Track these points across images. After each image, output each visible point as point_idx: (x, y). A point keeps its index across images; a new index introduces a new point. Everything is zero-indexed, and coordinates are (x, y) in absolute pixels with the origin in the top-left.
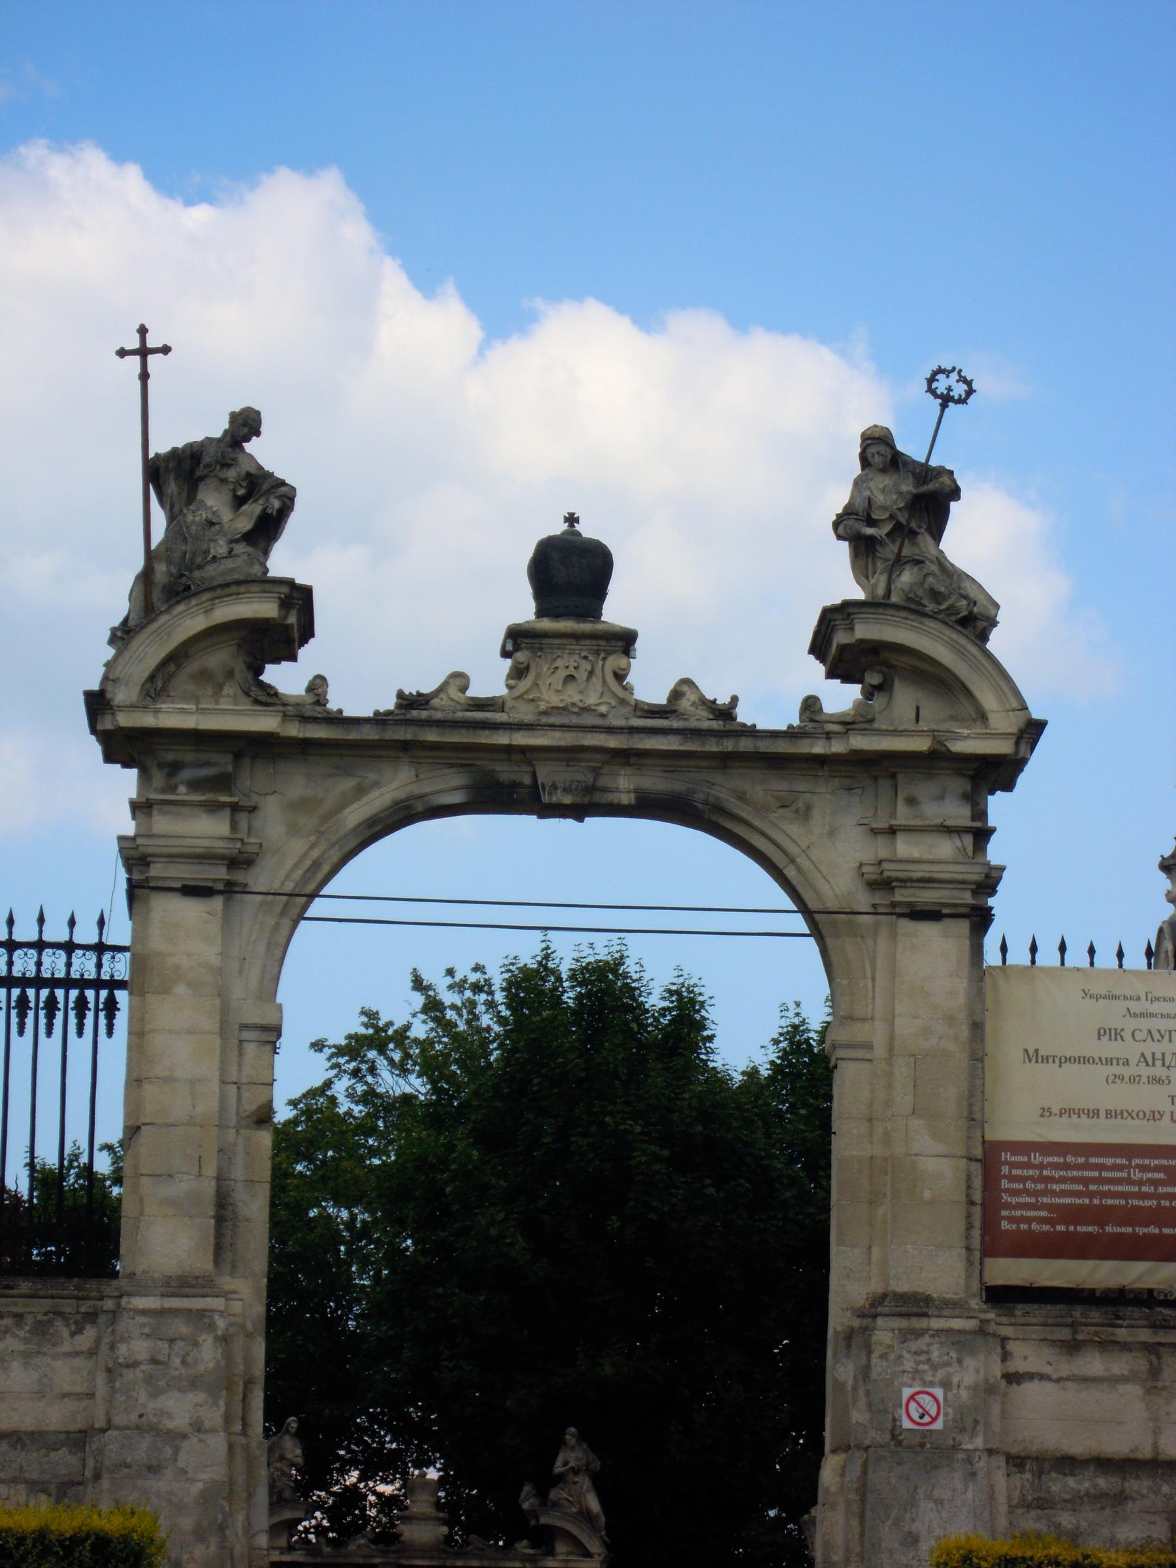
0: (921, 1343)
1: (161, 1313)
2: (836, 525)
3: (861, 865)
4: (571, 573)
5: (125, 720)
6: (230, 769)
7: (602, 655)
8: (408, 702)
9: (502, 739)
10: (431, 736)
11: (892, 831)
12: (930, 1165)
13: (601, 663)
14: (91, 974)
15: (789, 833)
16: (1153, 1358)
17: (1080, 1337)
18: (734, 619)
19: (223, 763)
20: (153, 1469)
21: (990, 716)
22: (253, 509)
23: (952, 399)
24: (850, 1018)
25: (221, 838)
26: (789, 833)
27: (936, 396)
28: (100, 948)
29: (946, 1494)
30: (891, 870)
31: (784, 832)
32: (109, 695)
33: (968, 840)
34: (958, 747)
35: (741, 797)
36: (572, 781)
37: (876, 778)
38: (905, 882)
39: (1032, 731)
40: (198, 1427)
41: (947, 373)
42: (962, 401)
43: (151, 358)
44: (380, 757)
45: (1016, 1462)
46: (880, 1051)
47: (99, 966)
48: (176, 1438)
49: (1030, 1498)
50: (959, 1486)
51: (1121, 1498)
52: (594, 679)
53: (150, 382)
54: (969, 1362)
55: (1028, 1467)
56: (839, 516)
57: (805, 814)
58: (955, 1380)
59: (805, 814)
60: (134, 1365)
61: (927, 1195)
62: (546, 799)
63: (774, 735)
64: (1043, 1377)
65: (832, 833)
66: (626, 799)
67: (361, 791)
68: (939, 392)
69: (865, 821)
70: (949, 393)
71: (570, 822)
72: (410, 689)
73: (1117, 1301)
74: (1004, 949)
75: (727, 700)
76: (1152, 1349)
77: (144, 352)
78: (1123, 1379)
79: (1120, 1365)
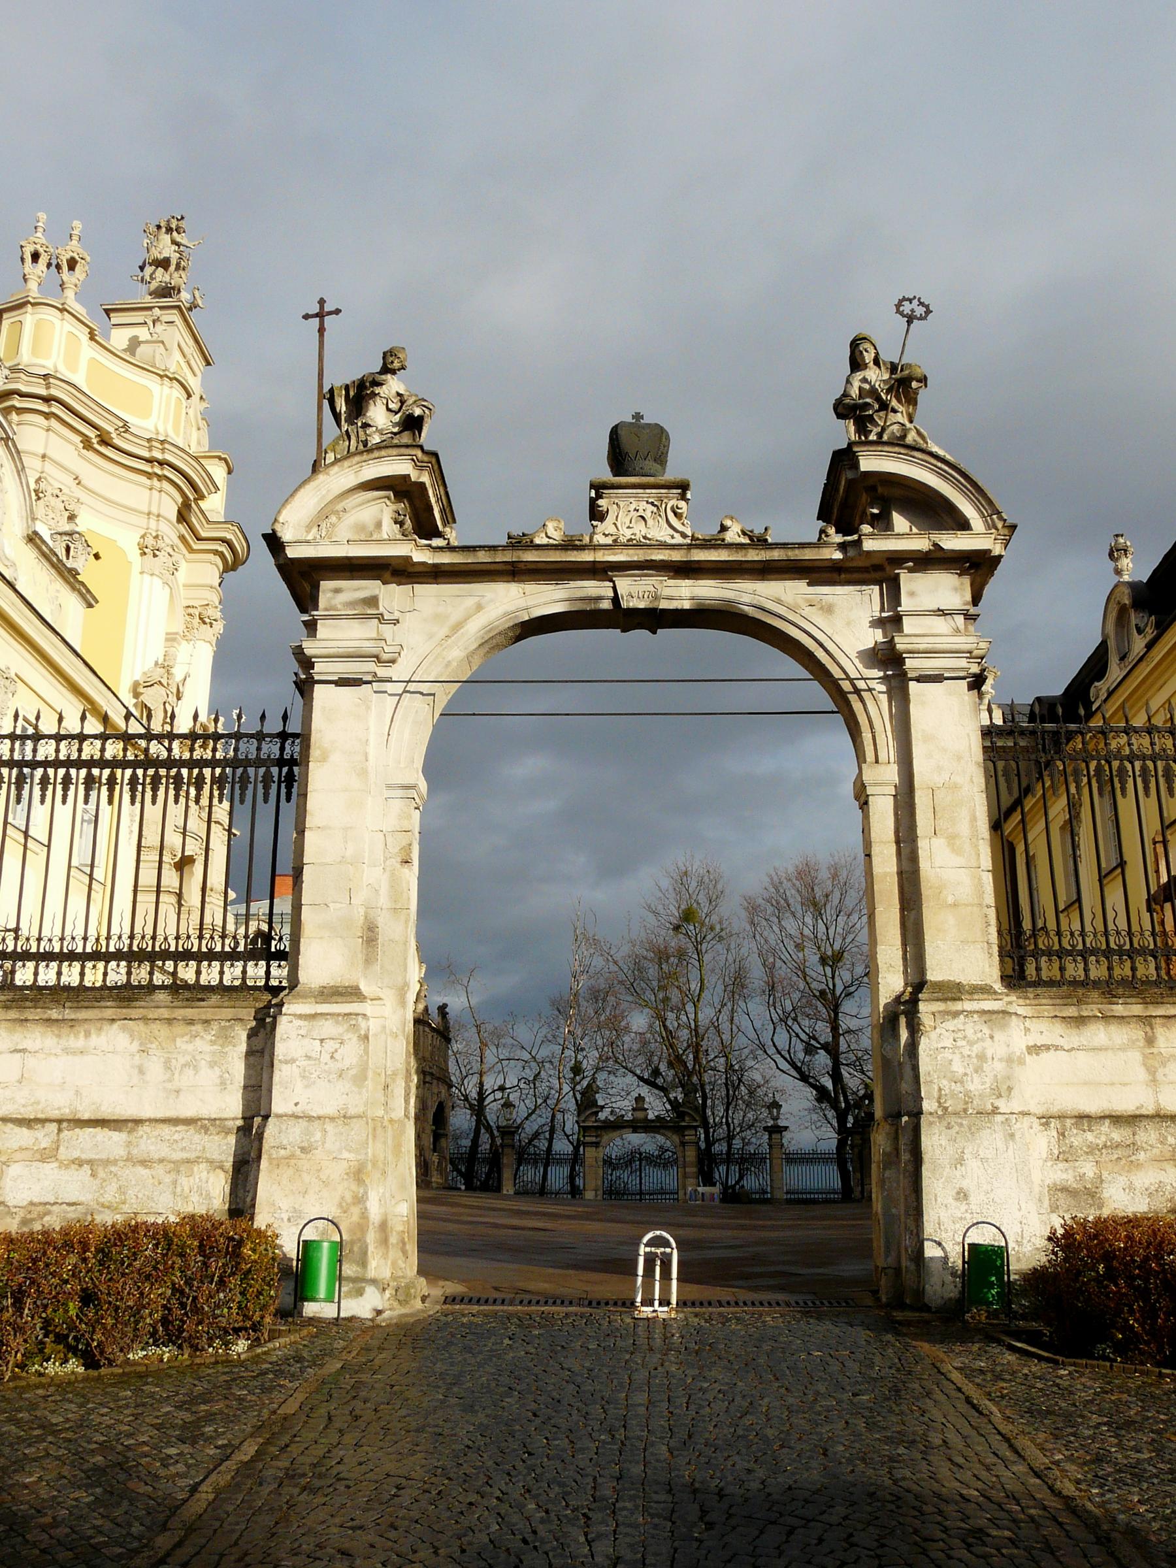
2: (835, 408)
5: (291, 553)
16: (1148, 1029)
17: (1085, 1014)
27: (904, 316)
28: (283, 736)
32: (279, 534)
33: (960, 620)
41: (910, 301)
42: (921, 318)
45: (1046, 1119)
47: (282, 749)
49: (1056, 1152)
50: (1001, 1145)
51: (1134, 1147)
54: (998, 1036)
55: (1052, 1125)
58: (989, 1054)
59: (828, 609)
60: (293, 1061)
61: (950, 900)
62: (624, 605)
63: (802, 546)
64: (1057, 1048)
66: (687, 605)
67: (479, 607)
71: (645, 633)
72: (516, 532)
76: (1146, 1020)
77: (321, 315)
78: (1123, 1049)
79: (1119, 1035)
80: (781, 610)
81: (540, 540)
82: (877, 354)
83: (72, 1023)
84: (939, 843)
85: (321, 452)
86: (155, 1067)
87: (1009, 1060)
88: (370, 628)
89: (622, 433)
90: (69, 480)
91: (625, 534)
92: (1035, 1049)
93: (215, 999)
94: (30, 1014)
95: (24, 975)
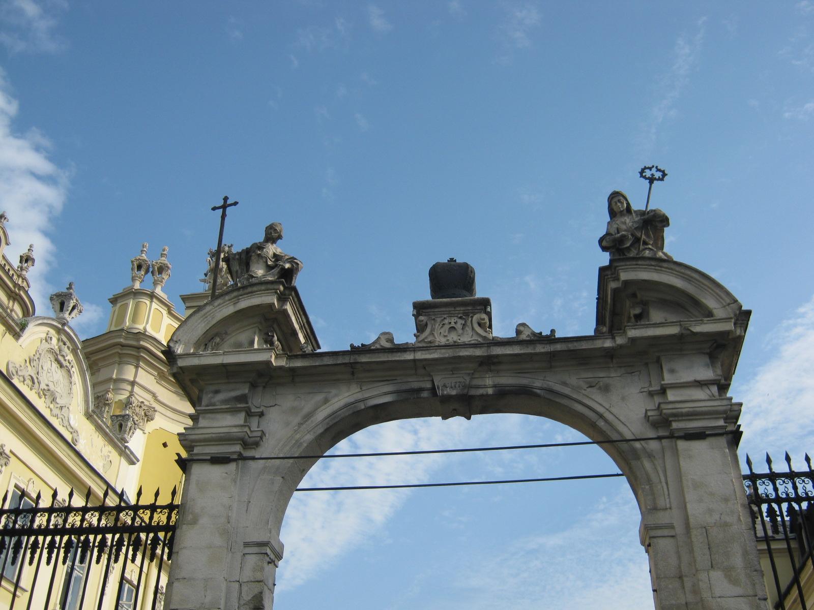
2: (601, 241)
3: (646, 411)
4: (452, 284)
5: (181, 363)
6: (246, 391)
7: (471, 315)
9: (409, 356)
10: (364, 359)
11: (663, 391)
13: (470, 319)
15: (597, 401)
19: (245, 390)
21: (715, 312)
23: (656, 179)
24: (655, 509)
25: (235, 426)
28: (171, 507)
30: (667, 409)
31: (593, 400)
33: (714, 389)
34: (698, 329)
36: (456, 382)
37: (647, 364)
38: (679, 416)
39: (744, 317)
41: (650, 169)
42: (659, 179)
43: (228, 209)
44: (338, 380)
46: (679, 529)
52: (467, 328)
53: (217, 206)
56: (601, 238)
59: (606, 389)
65: (623, 399)
66: (490, 391)
67: (326, 401)
68: (647, 176)
69: (645, 390)
70: (652, 176)
74: (749, 462)
75: (549, 333)
77: (224, 207)
80: (567, 391)
82: (628, 204)
84: (717, 576)
88: (240, 419)
90: (148, 397)
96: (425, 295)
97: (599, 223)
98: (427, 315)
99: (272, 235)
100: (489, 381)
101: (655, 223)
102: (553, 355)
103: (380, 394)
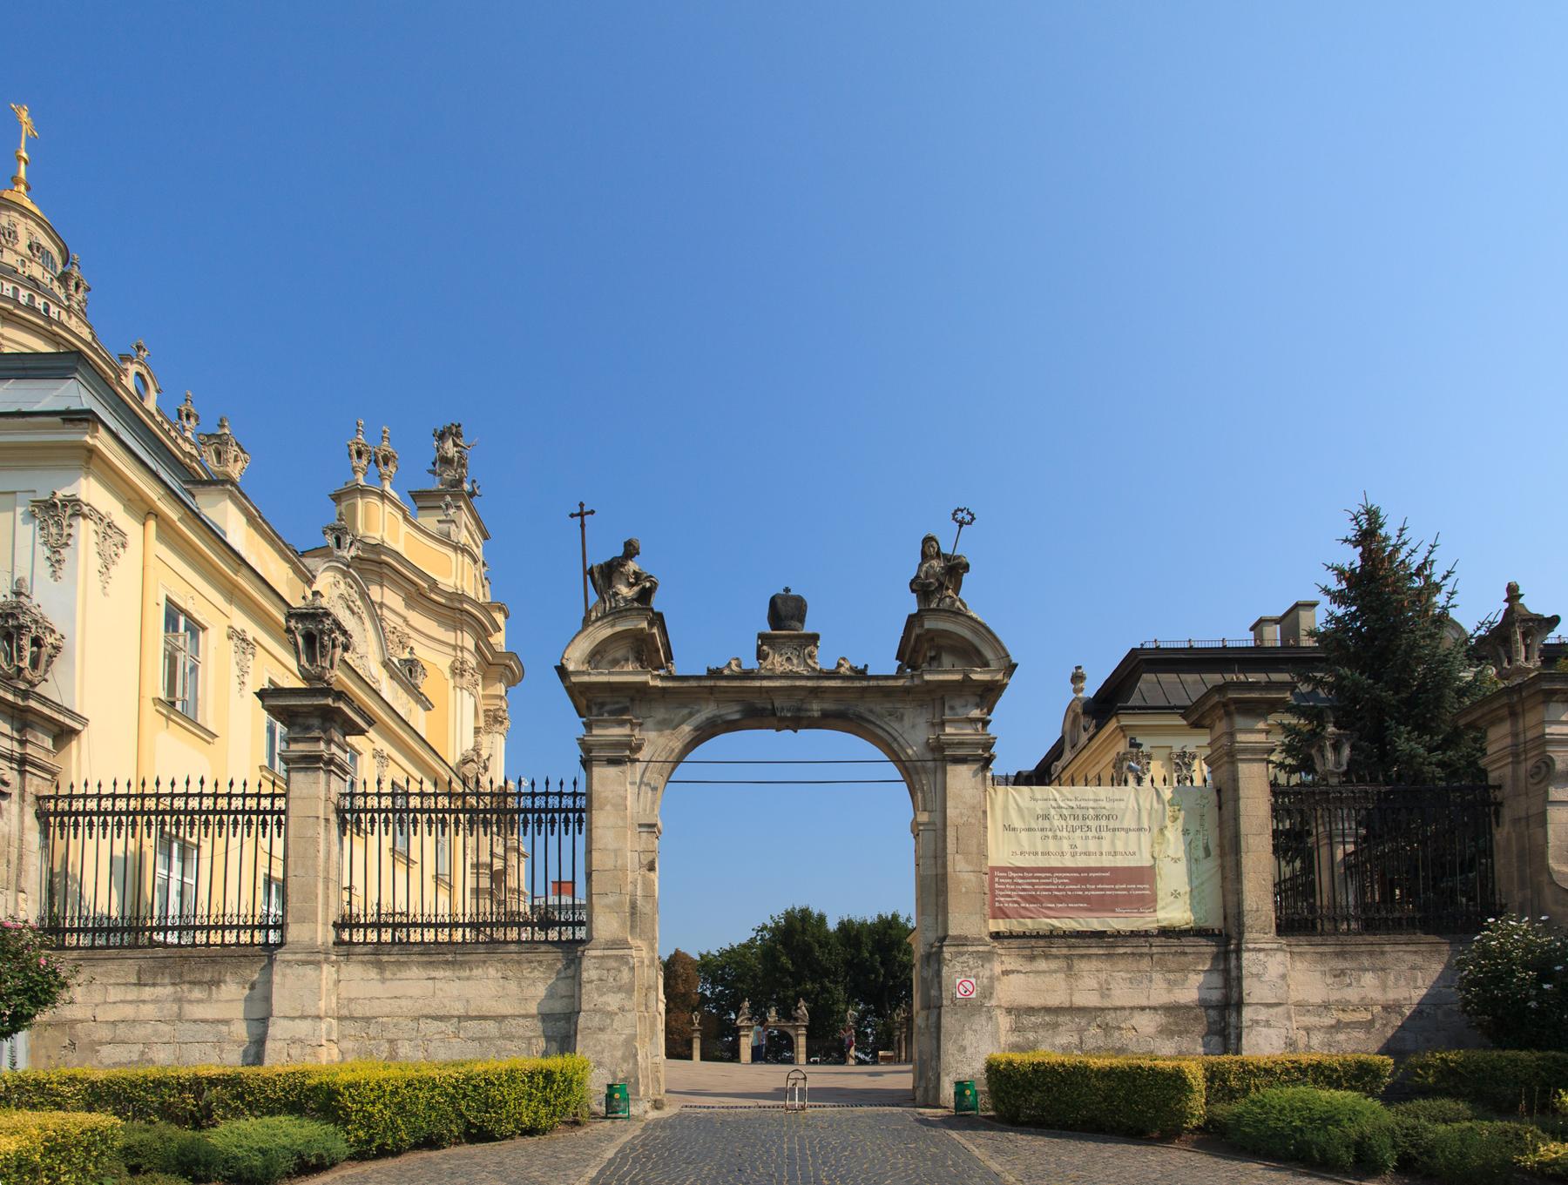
0: (964, 958)
1: (603, 957)
4: (786, 613)
8: (715, 674)
9: (757, 684)
10: (723, 683)
12: (965, 876)
14: (571, 805)
15: (894, 727)
18: (862, 632)
20: (601, 1030)
22: (636, 589)
26: (894, 727)
28: (575, 794)
29: (978, 1027)
35: (871, 711)
40: (622, 1009)
45: (1009, 1011)
48: (611, 1015)
57: (901, 719)
66: (816, 714)
72: (713, 667)
73: (1052, 936)
79: (1054, 965)
81: (726, 672)
83: (462, 964)
84: (958, 857)
85: (588, 612)
86: (512, 986)
87: (991, 978)
89: (779, 601)
91: (779, 669)
92: (1006, 973)
93: (543, 948)
94: (434, 958)
95: (415, 936)
96: (767, 630)
97: (910, 565)
98: (771, 647)
99: (631, 550)
100: (815, 707)
101: (956, 569)
102: (865, 689)
103: (732, 712)
